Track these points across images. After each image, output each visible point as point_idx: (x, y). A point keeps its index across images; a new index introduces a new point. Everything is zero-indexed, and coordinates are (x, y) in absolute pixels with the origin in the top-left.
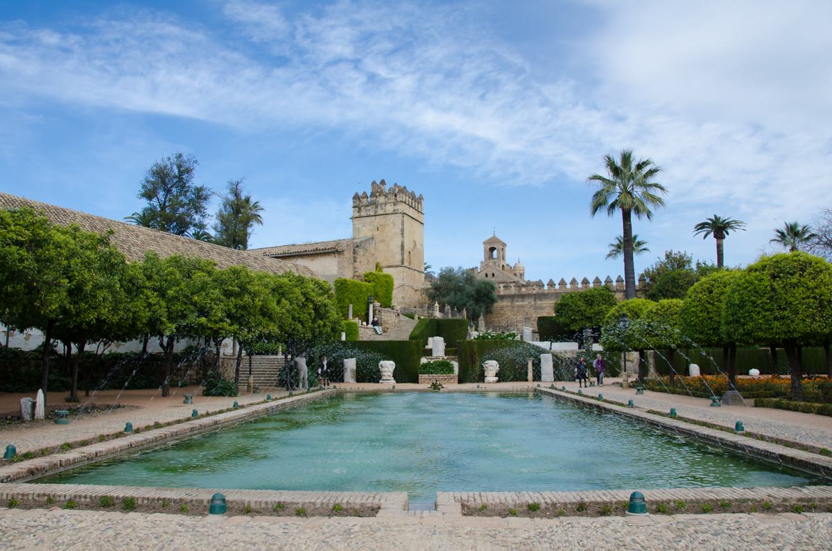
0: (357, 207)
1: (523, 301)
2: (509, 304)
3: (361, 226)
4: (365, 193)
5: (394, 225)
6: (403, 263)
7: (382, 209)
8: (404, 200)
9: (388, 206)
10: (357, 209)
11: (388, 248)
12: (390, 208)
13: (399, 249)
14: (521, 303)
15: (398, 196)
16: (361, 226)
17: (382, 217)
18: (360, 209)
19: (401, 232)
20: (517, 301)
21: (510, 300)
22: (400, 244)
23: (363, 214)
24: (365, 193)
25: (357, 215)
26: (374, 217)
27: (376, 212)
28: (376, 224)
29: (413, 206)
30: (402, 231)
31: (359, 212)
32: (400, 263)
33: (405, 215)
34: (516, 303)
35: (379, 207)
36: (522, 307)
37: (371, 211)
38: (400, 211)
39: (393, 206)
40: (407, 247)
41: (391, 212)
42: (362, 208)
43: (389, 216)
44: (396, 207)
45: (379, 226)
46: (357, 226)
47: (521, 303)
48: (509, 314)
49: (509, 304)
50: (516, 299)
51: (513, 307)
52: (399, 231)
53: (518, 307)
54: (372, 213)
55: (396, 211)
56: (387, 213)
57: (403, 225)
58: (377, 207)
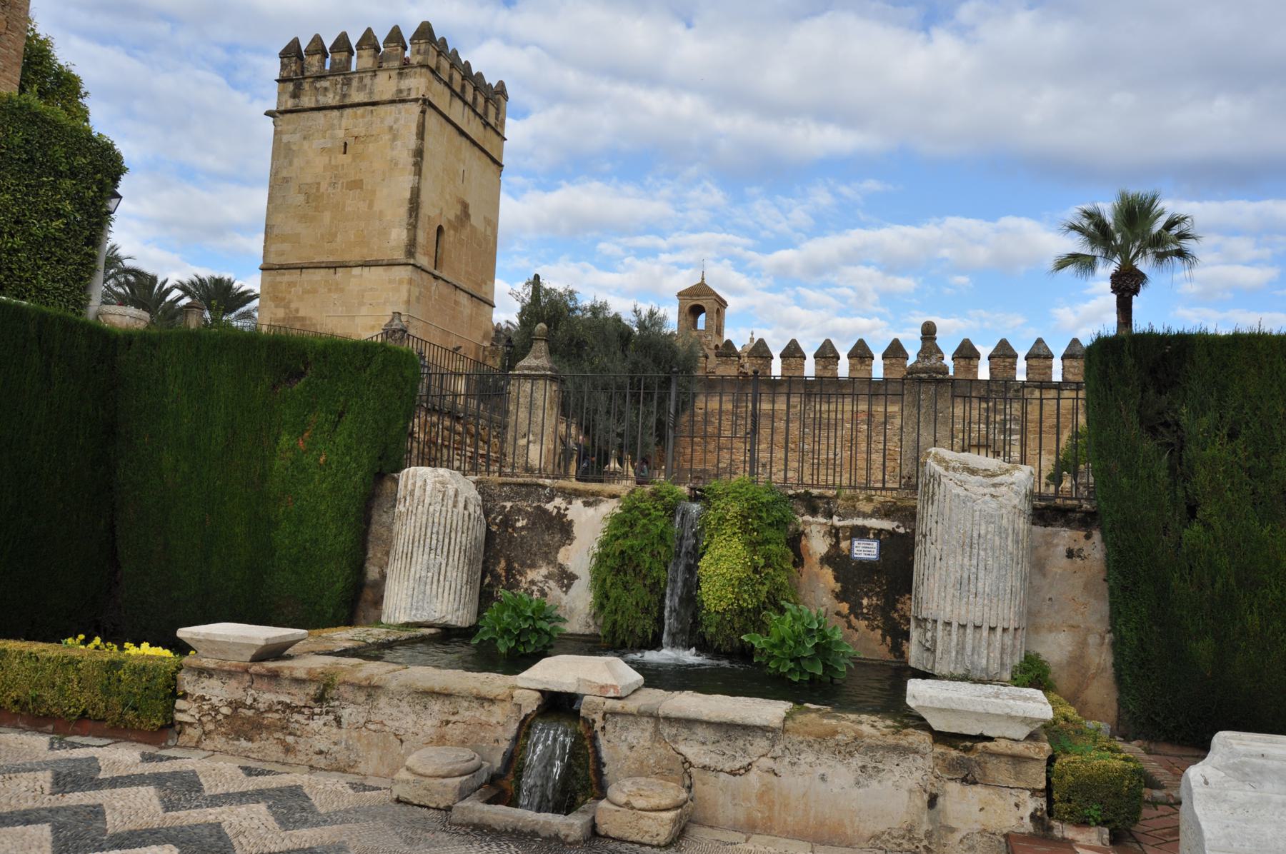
5: (395, 138)
7: (362, 88)
8: (433, 64)
9: (382, 77)
11: (370, 206)
12: (385, 85)
17: (360, 111)
19: (411, 160)
22: (408, 195)
26: (336, 113)
27: (344, 96)
28: (340, 133)
29: (469, 98)
30: (419, 153)
33: (430, 111)
35: (355, 83)
37: (331, 95)
38: (413, 96)
40: (429, 208)
41: (387, 97)
44: (406, 83)
45: (351, 141)
52: (406, 159)
54: (331, 99)
55: (404, 95)
56: (376, 98)
57: (421, 134)
58: (348, 83)
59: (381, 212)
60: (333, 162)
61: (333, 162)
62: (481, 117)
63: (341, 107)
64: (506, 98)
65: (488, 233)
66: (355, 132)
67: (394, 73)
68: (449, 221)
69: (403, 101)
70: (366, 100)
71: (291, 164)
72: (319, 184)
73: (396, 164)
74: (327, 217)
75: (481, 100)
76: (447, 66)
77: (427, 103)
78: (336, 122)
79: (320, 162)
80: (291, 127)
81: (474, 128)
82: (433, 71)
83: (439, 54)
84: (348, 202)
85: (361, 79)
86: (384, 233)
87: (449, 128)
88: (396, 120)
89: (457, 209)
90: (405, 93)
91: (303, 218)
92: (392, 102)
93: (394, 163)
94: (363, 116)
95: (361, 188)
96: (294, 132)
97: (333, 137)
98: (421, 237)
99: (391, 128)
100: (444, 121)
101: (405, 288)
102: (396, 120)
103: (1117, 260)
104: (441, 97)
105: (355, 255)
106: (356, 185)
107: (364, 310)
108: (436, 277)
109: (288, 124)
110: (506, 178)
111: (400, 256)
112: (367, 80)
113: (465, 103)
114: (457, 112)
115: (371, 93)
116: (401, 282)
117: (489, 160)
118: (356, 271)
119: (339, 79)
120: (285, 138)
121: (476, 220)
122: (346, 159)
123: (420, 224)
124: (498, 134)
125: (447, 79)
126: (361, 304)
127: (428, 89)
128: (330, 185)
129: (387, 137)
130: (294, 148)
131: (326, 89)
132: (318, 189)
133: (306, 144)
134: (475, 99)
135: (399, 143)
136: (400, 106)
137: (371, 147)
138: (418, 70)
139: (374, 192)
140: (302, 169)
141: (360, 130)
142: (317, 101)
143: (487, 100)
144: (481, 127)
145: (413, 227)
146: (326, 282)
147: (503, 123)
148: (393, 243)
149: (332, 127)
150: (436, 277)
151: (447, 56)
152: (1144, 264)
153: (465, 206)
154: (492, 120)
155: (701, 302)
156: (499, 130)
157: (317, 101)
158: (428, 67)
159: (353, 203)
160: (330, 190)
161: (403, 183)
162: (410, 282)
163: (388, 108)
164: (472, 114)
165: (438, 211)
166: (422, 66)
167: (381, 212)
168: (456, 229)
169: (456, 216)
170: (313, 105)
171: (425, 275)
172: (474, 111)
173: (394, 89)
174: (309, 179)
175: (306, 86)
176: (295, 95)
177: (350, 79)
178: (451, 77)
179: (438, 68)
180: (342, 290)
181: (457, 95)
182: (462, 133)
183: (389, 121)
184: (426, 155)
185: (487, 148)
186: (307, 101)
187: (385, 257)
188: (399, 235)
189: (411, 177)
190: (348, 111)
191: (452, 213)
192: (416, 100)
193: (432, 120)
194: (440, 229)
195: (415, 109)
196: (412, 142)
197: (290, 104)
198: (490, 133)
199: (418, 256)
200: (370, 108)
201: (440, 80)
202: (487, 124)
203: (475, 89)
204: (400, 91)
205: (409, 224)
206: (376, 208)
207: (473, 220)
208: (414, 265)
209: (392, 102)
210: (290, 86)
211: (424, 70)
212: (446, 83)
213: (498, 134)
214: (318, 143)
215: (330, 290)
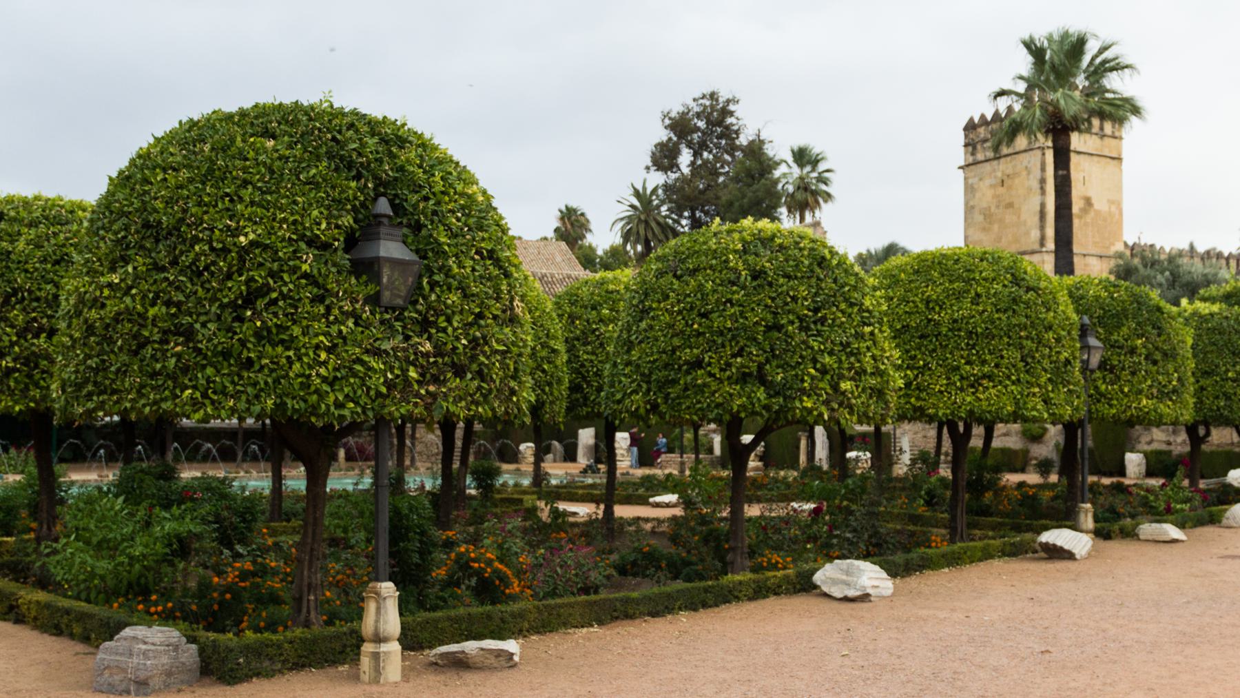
0: (970, 145)
3: (976, 179)
4: (983, 116)
5: (1029, 173)
6: (1042, 244)
10: (970, 149)
13: (1037, 218)
16: (976, 179)
18: (974, 148)
22: (1038, 208)
23: (980, 157)
24: (983, 116)
25: (971, 159)
26: (995, 162)
28: (999, 174)
31: (973, 154)
32: (1036, 247)
42: (979, 147)
46: (970, 181)
52: (1035, 185)
74: (996, 227)
79: (989, 193)
93: (1030, 189)
106: (1010, 205)
122: (1001, 190)
129: (1024, 173)
137: (1017, 181)
141: (1008, 172)
149: (994, 171)
159: (1009, 217)
214: (988, 182)
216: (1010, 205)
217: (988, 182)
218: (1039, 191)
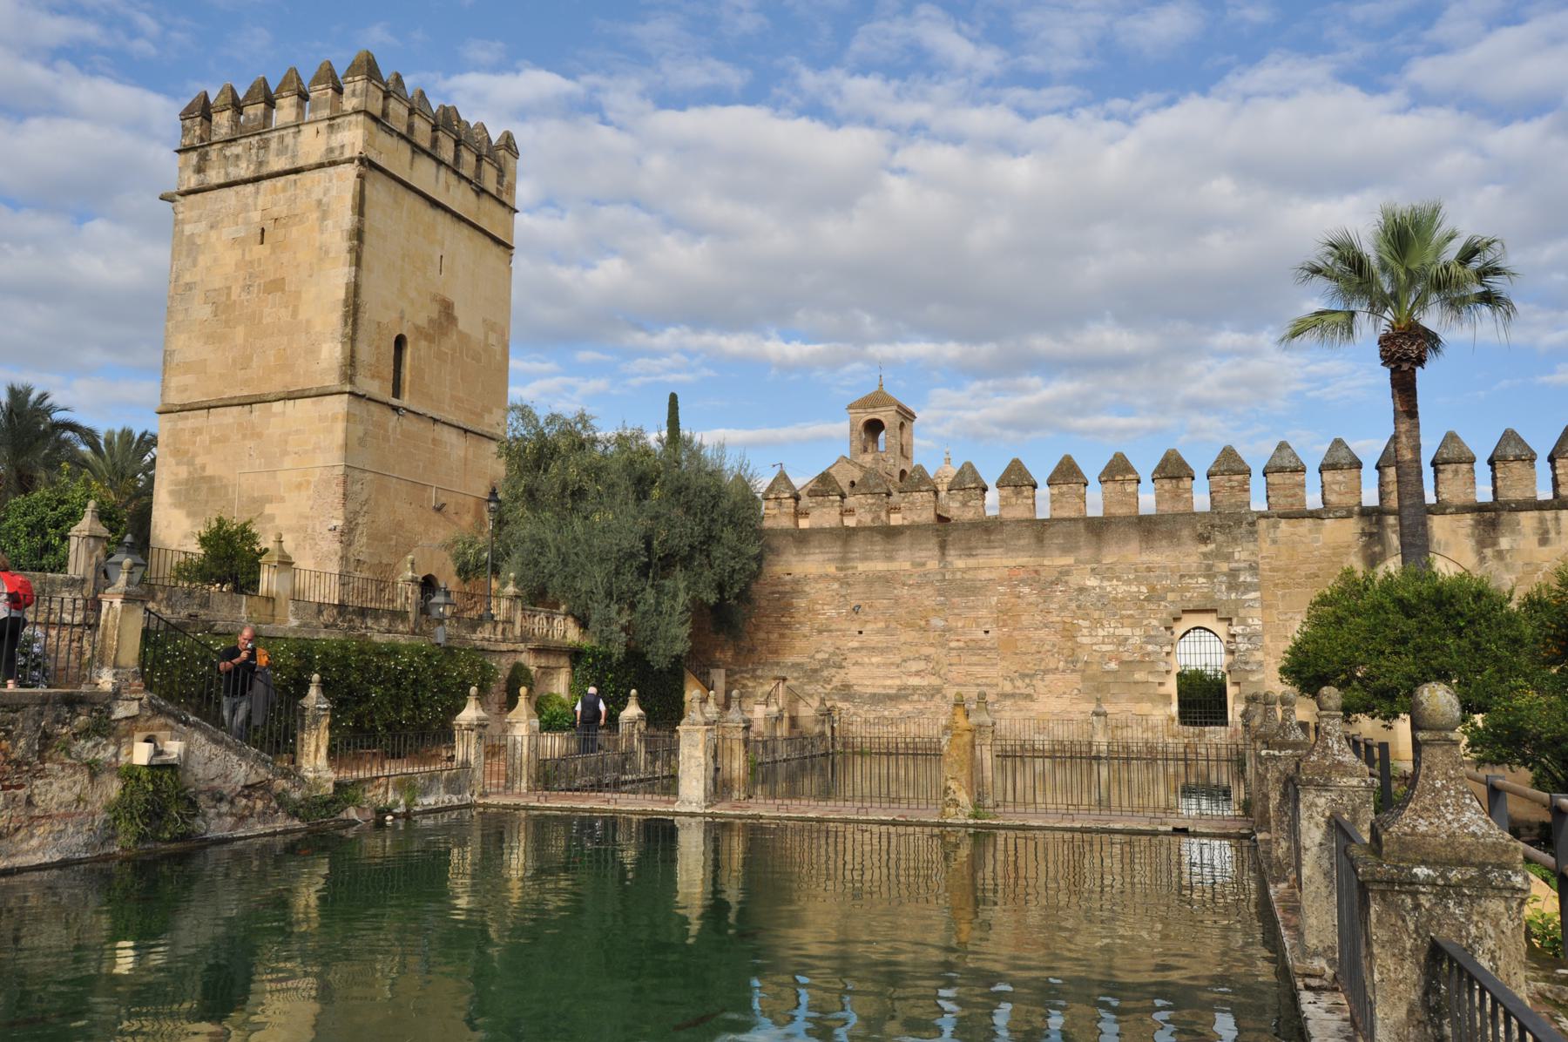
1: (890, 558)
2: (831, 569)
5: (324, 216)
9: (308, 131)
11: (295, 314)
12: (311, 144)
14: (880, 566)
15: (347, 89)
17: (280, 182)
19: (345, 245)
20: (865, 558)
21: (837, 549)
22: (341, 294)
26: (250, 188)
27: (260, 164)
28: (256, 216)
30: (358, 234)
33: (373, 175)
34: (861, 567)
35: (274, 145)
36: (887, 580)
37: (243, 165)
38: (347, 155)
39: (323, 138)
40: (382, 313)
41: (314, 159)
43: (306, 174)
45: (269, 225)
47: (880, 566)
48: (833, 613)
49: (831, 569)
50: (858, 546)
51: (845, 583)
52: (339, 243)
53: (871, 580)
55: (336, 156)
56: (300, 163)
57: (360, 207)
58: (265, 146)
59: (308, 321)
60: (247, 257)
61: (247, 257)
62: (470, 182)
63: (256, 180)
64: (516, 155)
65: (493, 339)
66: (275, 212)
67: (323, 125)
68: (417, 328)
69: (333, 163)
70: (288, 167)
71: (195, 264)
72: (229, 288)
73: (327, 253)
75: (468, 158)
76: (404, 112)
77: (367, 163)
78: (250, 200)
79: (230, 258)
80: (195, 213)
81: (459, 197)
82: (374, 119)
83: (387, 95)
84: (267, 311)
85: (282, 138)
86: (312, 350)
87: (410, 200)
88: (326, 191)
89: (434, 311)
90: (337, 153)
91: (211, 338)
92: (320, 166)
93: (324, 251)
94: (284, 190)
95: (283, 290)
96: (199, 220)
97: (247, 223)
98: (364, 353)
99: (319, 202)
100: (400, 187)
101: (340, 427)
102: (326, 191)
103: (1389, 315)
104: (394, 156)
105: (275, 386)
106: (277, 285)
107: (288, 463)
108: (395, 409)
109: (191, 209)
110: (520, 262)
111: (332, 381)
112: (289, 140)
113: (440, 162)
114: (425, 175)
115: (294, 156)
116: (334, 419)
117: (488, 241)
118: (277, 407)
119: (254, 140)
120: (188, 229)
121: (468, 320)
122: (264, 250)
123: (361, 335)
124: (504, 204)
125: (404, 130)
126: (285, 453)
127: (368, 143)
128: (243, 288)
129: (315, 215)
130: (199, 241)
131: (237, 156)
132: (229, 295)
133: (214, 234)
134: (457, 156)
135: (330, 223)
136: (331, 170)
137: (295, 232)
138: (353, 118)
139: (298, 294)
140: (208, 269)
141: (280, 210)
142: (227, 174)
143: (479, 159)
144: (472, 196)
145: (352, 339)
146: (240, 425)
147: (511, 188)
148: (324, 365)
149: (245, 208)
150: (395, 409)
151: (402, 98)
152: (1432, 318)
153: (447, 308)
154: (491, 186)
155: (880, 414)
156: (504, 198)
157: (227, 174)
158: (366, 113)
159: (273, 312)
160: (244, 296)
161: (338, 276)
162: (349, 417)
163: (316, 174)
164: (453, 179)
165: (395, 316)
166: (357, 112)
167: (308, 321)
168: (430, 338)
169: (431, 321)
170: (222, 181)
171: (373, 407)
172: (456, 173)
173: (323, 149)
174: (218, 283)
175: (213, 153)
176: (200, 170)
177: (268, 140)
178: (411, 127)
179: (385, 113)
180: (260, 436)
181: (424, 151)
182: (435, 204)
183: (317, 193)
184: (368, 237)
185: (483, 224)
186: (214, 176)
187: (314, 384)
188: (331, 352)
189: (346, 269)
190: (266, 184)
191: (423, 314)
192: (351, 160)
193: (378, 191)
194: (400, 342)
195: (351, 171)
196: (345, 218)
197: (193, 181)
198: (487, 204)
199: (359, 379)
200: (292, 177)
201: (390, 131)
202: (480, 191)
203: (458, 143)
204: (331, 150)
205: (344, 336)
206: (302, 316)
207: (462, 324)
208: (351, 393)
209: (320, 166)
210: (193, 157)
211: (361, 117)
212: (401, 136)
213: (504, 204)
214: (228, 232)
215: (244, 437)
216: (277, 285)
217: (228, 232)
218: (345, 257)
